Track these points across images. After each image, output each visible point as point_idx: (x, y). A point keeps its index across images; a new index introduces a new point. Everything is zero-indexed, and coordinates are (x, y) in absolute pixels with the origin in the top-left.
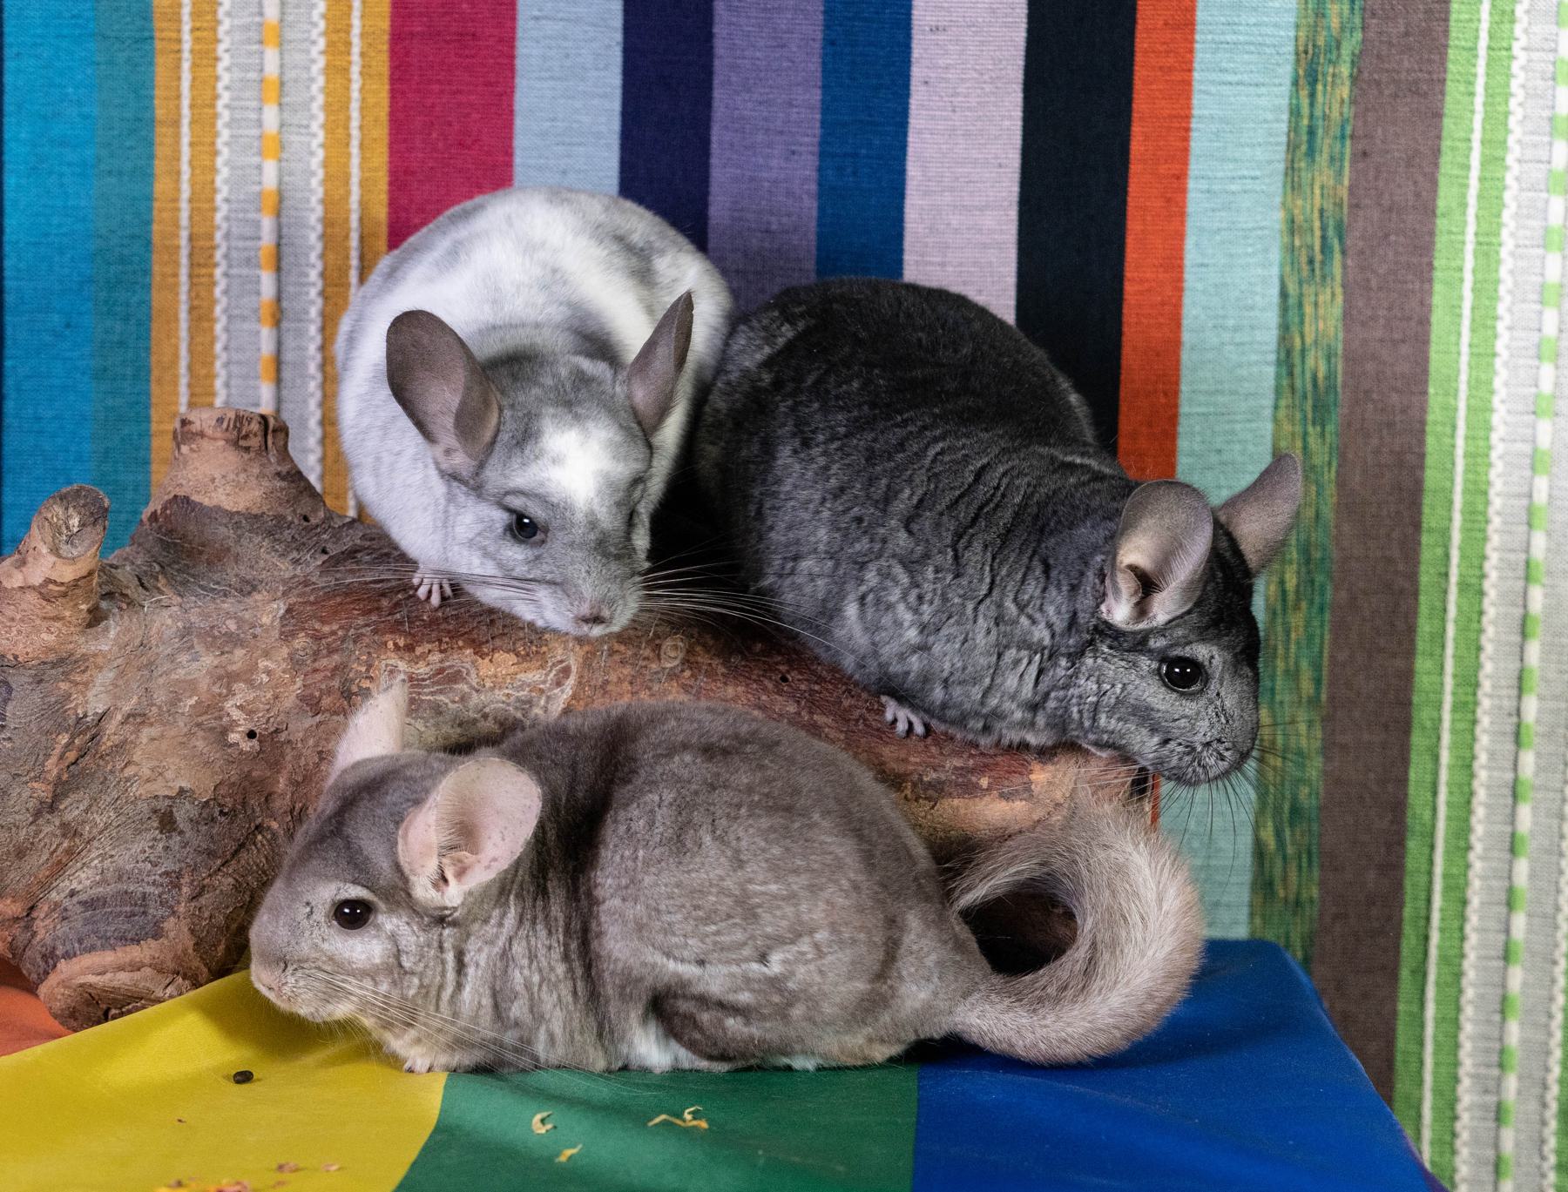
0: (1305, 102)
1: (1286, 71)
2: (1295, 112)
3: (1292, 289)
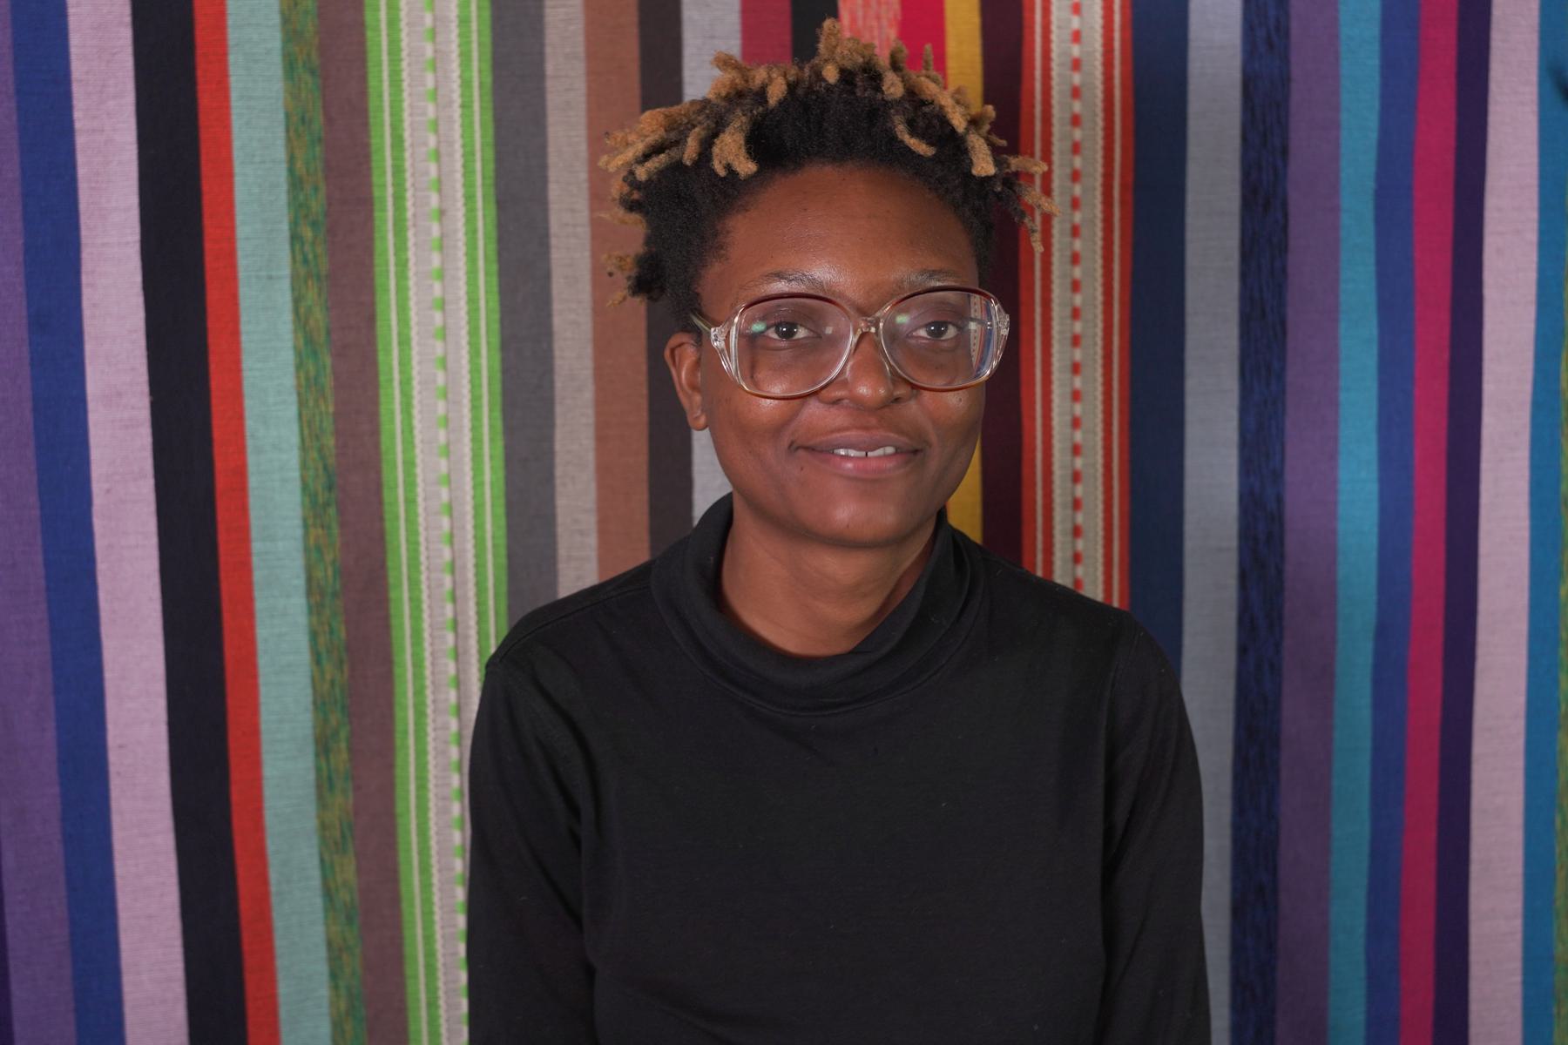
0: (324, 765)
1: (310, 749)
2: (318, 770)
3: (327, 857)
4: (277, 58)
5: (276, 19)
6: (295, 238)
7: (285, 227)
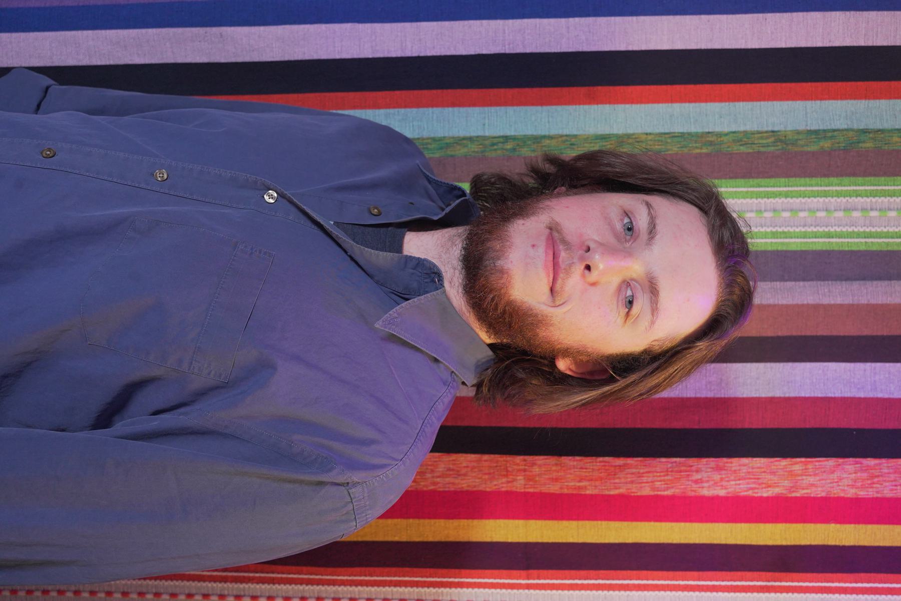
4: (606, 130)
5: (630, 131)
6: (506, 139)
7: (511, 132)
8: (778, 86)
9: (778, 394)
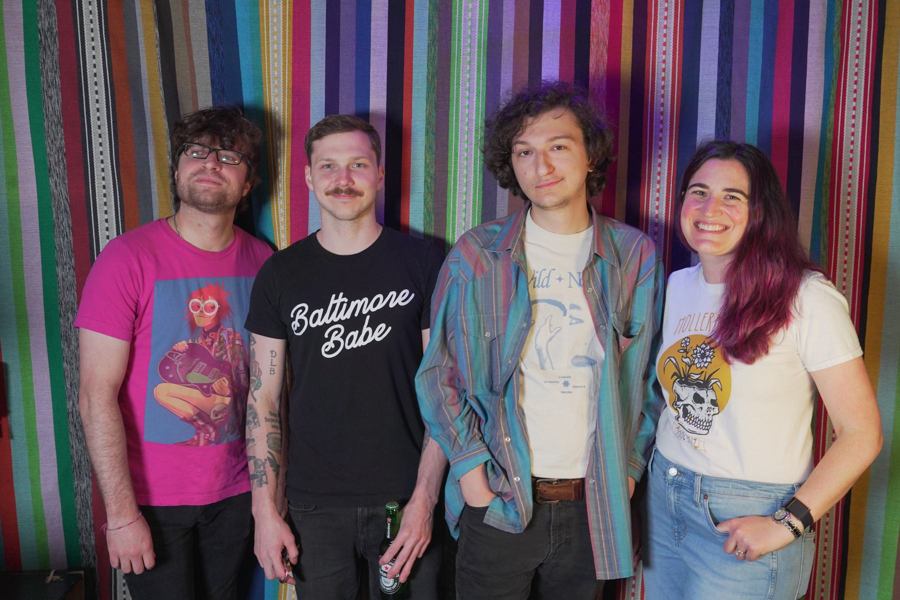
8: (406, 44)
9: (558, 48)
